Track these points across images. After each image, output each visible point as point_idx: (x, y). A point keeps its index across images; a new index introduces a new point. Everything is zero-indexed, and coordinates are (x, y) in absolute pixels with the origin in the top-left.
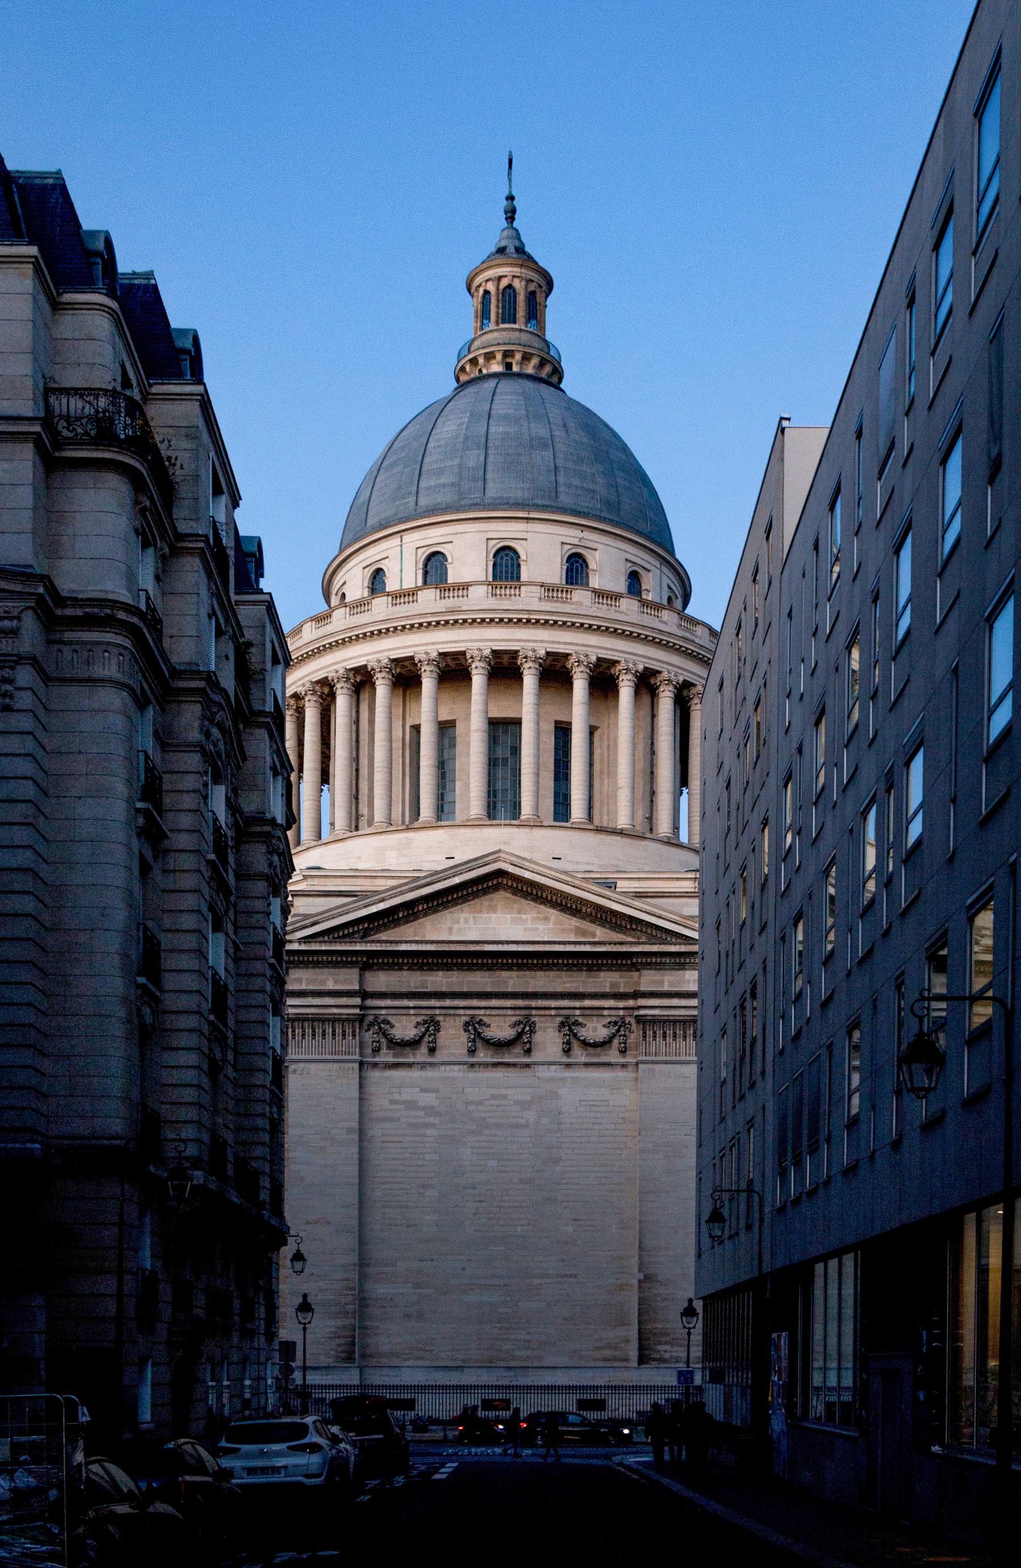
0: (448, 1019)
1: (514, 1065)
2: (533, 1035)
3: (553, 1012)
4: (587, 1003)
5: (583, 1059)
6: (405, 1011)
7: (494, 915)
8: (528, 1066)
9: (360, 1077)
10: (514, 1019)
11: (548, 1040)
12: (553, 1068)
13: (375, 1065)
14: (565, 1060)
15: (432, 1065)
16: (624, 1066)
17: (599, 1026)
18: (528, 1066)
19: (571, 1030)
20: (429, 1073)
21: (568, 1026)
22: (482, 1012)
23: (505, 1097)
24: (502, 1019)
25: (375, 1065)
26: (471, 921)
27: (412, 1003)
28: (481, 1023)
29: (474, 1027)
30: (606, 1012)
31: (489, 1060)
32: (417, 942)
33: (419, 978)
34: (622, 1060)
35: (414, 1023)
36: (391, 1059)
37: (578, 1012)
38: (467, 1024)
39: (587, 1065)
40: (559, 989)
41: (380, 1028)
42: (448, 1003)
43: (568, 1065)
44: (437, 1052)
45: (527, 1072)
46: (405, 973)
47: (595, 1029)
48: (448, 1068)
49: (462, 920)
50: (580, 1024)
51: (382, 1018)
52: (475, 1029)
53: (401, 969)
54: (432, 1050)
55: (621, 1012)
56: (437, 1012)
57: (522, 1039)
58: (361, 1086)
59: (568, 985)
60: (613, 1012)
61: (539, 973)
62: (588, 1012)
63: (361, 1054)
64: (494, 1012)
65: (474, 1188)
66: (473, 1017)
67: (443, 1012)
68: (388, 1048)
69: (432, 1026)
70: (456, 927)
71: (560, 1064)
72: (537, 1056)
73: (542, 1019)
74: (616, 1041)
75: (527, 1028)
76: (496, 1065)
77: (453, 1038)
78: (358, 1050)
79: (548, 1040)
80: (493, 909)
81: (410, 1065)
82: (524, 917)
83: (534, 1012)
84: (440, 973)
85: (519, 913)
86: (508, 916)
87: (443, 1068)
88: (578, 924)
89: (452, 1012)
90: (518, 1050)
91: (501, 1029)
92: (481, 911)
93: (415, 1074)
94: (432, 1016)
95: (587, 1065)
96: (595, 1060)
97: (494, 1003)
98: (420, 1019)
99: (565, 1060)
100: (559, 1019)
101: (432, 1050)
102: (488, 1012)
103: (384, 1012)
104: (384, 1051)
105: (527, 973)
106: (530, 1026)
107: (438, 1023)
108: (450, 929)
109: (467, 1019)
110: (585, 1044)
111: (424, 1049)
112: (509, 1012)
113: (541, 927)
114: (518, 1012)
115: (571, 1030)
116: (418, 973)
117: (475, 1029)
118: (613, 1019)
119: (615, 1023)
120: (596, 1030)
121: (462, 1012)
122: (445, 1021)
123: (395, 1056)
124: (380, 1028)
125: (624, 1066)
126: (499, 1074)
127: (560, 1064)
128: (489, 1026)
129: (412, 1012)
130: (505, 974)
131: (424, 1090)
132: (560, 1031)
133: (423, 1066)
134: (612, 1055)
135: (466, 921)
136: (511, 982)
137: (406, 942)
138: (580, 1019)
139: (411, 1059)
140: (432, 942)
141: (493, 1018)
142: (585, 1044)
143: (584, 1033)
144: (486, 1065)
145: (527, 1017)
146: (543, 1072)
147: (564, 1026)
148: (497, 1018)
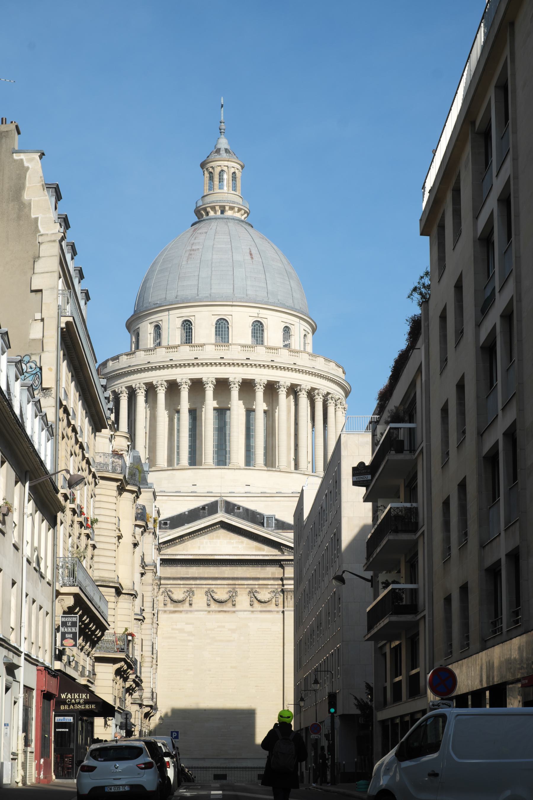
0: (198, 589)
1: (228, 611)
2: (237, 598)
3: (246, 586)
4: (261, 582)
5: (260, 609)
8: (234, 612)
10: (228, 590)
11: (243, 599)
12: (246, 613)
13: (165, 611)
15: (191, 611)
16: (278, 612)
17: (267, 593)
18: (234, 612)
19: (254, 595)
20: (190, 615)
21: (252, 593)
22: (213, 586)
24: (222, 589)
25: (165, 611)
28: (213, 591)
29: (209, 593)
30: (269, 587)
31: (217, 609)
32: (185, 555)
36: (172, 609)
37: (257, 586)
38: (206, 592)
39: (261, 611)
40: (248, 576)
41: (168, 594)
42: (198, 582)
43: (252, 612)
44: (193, 605)
45: (234, 615)
47: (265, 595)
48: (198, 613)
50: (258, 592)
51: (168, 589)
54: (191, 605)
55: (276, 587)
56: (193, 586)
57: (231, 600)
60: (273, 587)
62: (261, 586)
65: (210, 671)
66: (209, 588)
67: (196, 586)
68: (171, 603)
69: (191, 592)
71: (249, 611)
72: (238, 607)
73: (241, 589)
74: (274, 600)
76: (220, 611)
77: (200, 599)
79: (243, 599)
80: (218, 537)
81: (181, 612)
82: (232, 541)
83: (237, 586)
87: (196, 613)
89: (200, 586)
90: (230, 604)
91: (222, 594)
92: (213, 539)
93: (183, 616)
94: (191, 588)
95: (261, 611)
96: (264, 609)
98: (185, 590)
99: (251, 609)
100: (249, 590)
101: (191, 605)
102: (216, 586)
103: (169, 586)
107: (193, 591)
108: (199, 547)
109: (207, 590)
110: (260, 601)
112: (226, 586)
113: (240, 546)
114: (230, 586)
115: (254, 595)
117: (210, 594)
118: (273, 590)
119: (274, 591)
120: (264, 595)
121: (204, 586)
122: (197, 590)
123: (174, 607)
124: (168, 594)
125: (278, 612)
126: (221, 616)
127: (249, 611)
129: (182, 586)
131: (187, 624)
133: (187, 612)
134: (272, 607)
137: (180, 555)
138: (258, 590)
139: (181, 609)
140: (191, 555)
142: (260, 601)
143: (259, 597)
144: (216, 611)
145: (234, 589)
146: (241, 615)
148: (220, 589)
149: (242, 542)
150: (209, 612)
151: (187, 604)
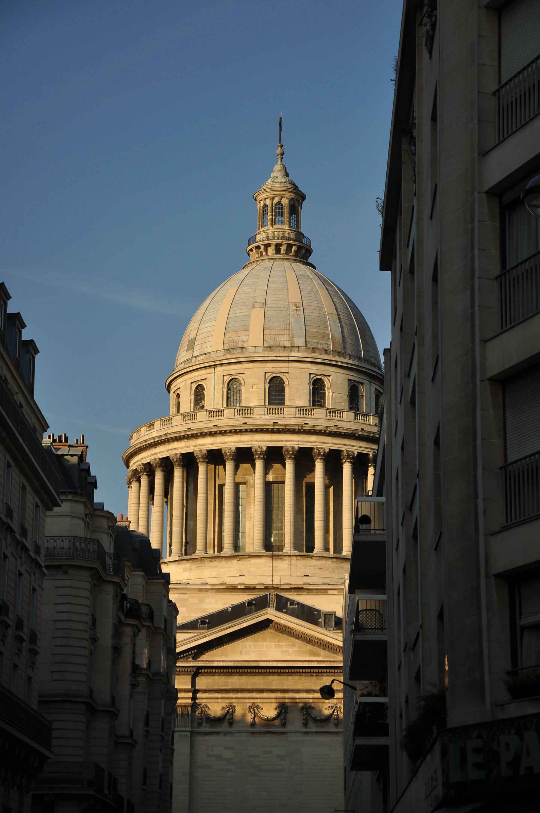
5: (314, 729)
6: (216, 700)
7: (265, 643)
8: (284, 733)
9: (191, 740)
13: (199, 733)
14: (304, 730)
15: (231, 733)
16: (337, 733)
18: (284, 733)
20: (229, 738)
22: (258, 700)
23: (271, 752)
24: (269, 705)
25: (199, 733)
26: (253, 647)
27: (220, 696)
33: (224, 680)
34: (335, 730)
35: (221, 707)
36: (208, 730)
39: (317, 733)
40: (301, 687)
43: (306, 733)
44: (234, 725)
46: (216, 677)
49: (248, 646)
51: (203, 704)
52: (254, 710)
53: (214, 675)
56: (234, 700)
58: (192, 746)
59: (305, 685)
61: (290, 677)
63: (192, 727)
64: (265, 701)
66: (253, 703)
67: (237, 700)
68: (207, 723)
70: (244, 650)
75: (283, 711)
78: (190, 724)
80: (264, 639)
81: (218, 733)
82: (281, 644)
84: (236, 677)
85: (279, 641)
86: (273, 644)
88: (310, 648)
89: (242, 700)
92: (258, 641)
93: (221, 738)
94: (231, 703)
95: (317, 733)
96: (320, 730)
97: (265, 695)
98: (224, 705)
102: (262, 700)
104: (204, 724)
105: (283, 677)
106: (285, 709)
108: (241, 652)
109: (250, 705)
111: (226, 724)
113: (290, 650)
116: (224, 677)
119: (332, 707)
121: (247, 700)
123: (210, 727)
125: (337, 733)
128: (262, 709)
129: (220, 700)
130: (271, 678)
131: (226, 748)
132: (301, 712)
133: (226, 733)
135: (250, 646)
136: (274, 683)
141: (264, 704)
147: (304, 709)
148: (267, 704)
149: (293, 645)
150: (253, 733)
151: (226, 724)
